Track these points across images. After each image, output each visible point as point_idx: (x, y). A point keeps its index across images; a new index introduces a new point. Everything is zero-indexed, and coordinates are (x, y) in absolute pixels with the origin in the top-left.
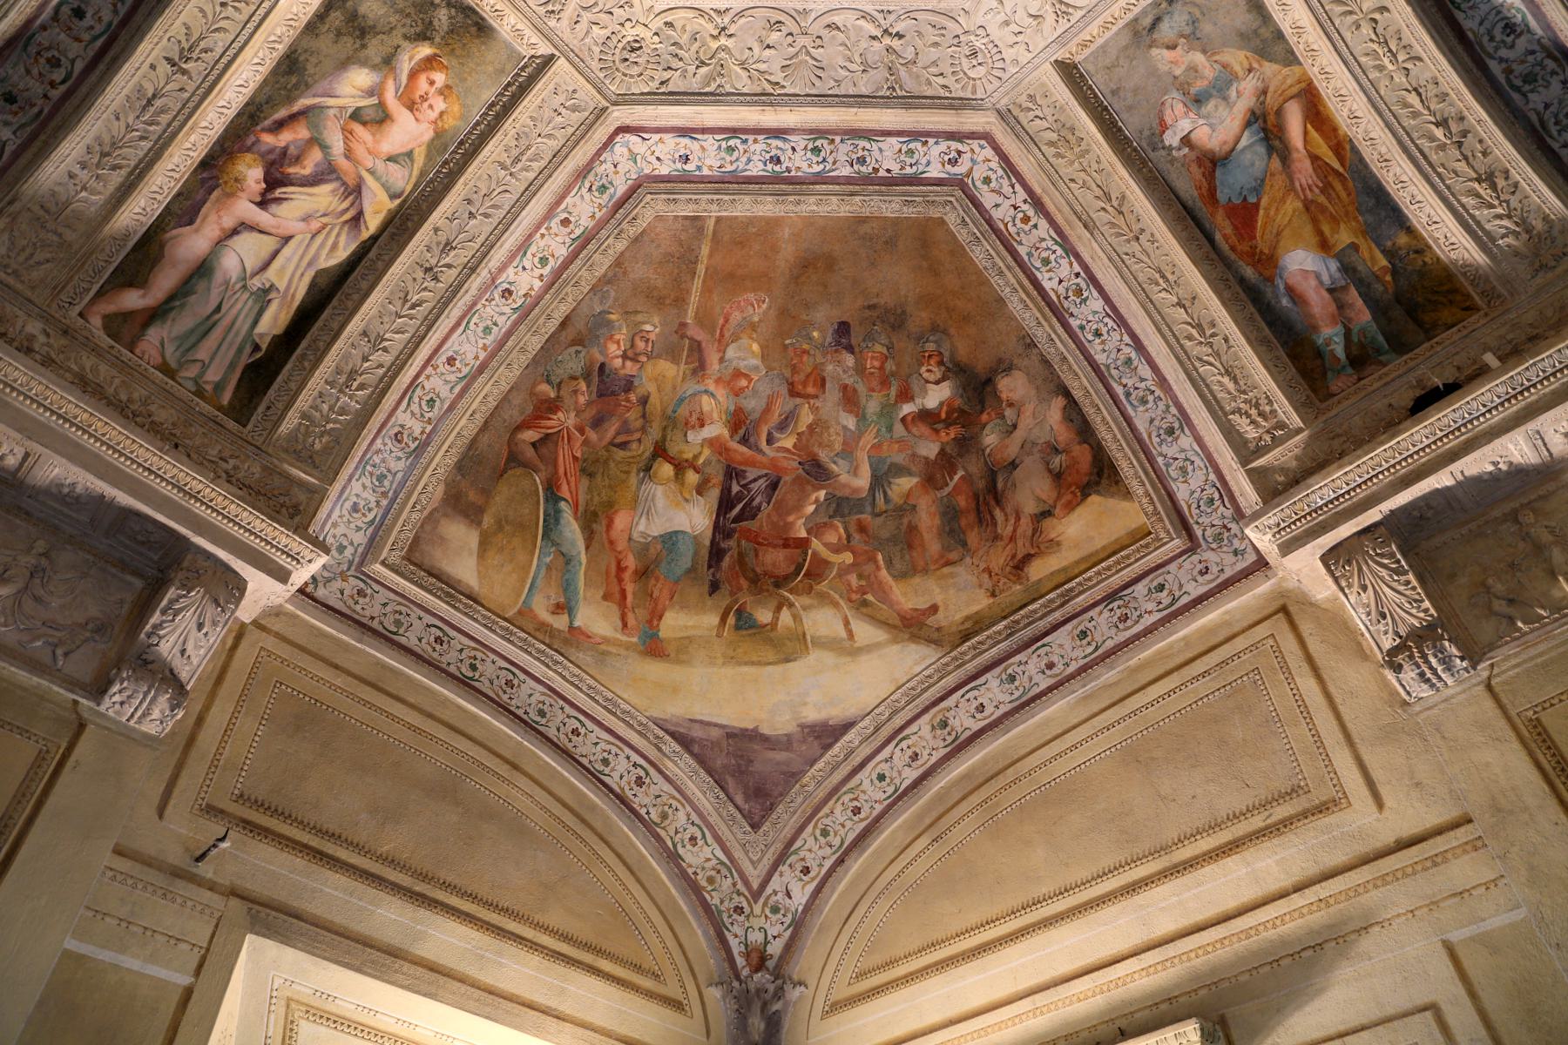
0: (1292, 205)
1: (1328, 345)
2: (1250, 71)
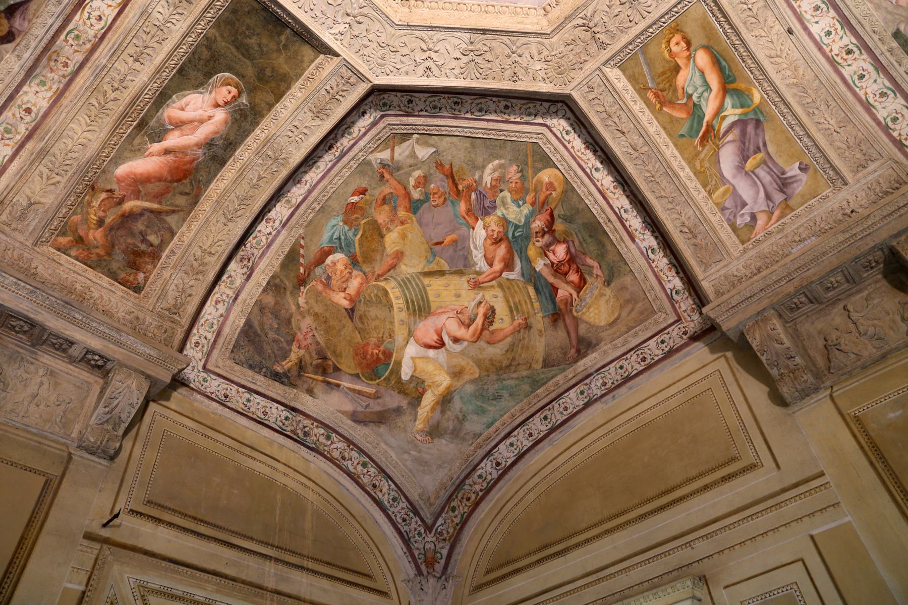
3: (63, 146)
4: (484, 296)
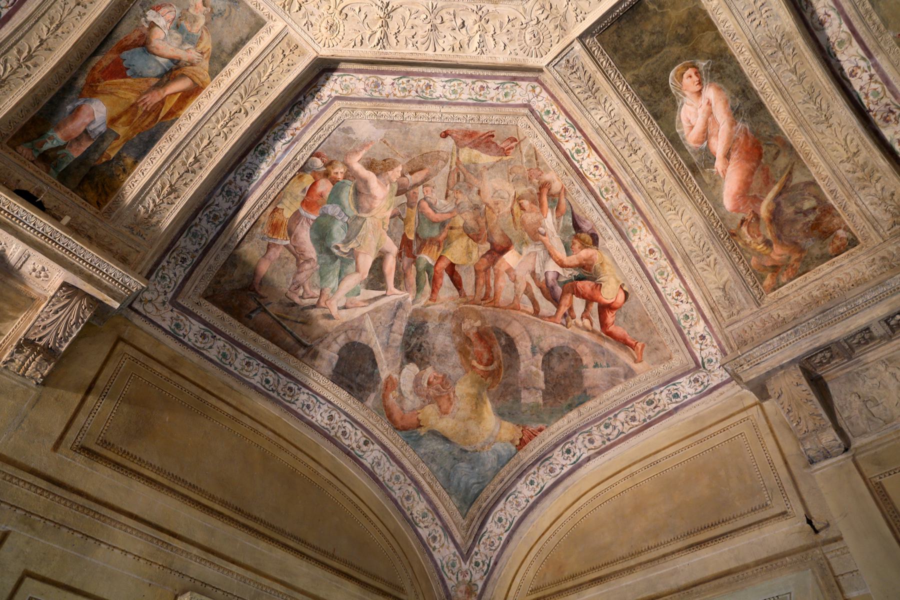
0: (132, 97)
1: (49, 138)
2: (202, 53)
3: (687, 241)
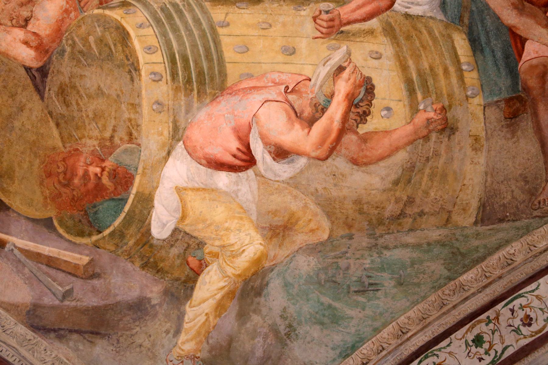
4: (349, 53)
